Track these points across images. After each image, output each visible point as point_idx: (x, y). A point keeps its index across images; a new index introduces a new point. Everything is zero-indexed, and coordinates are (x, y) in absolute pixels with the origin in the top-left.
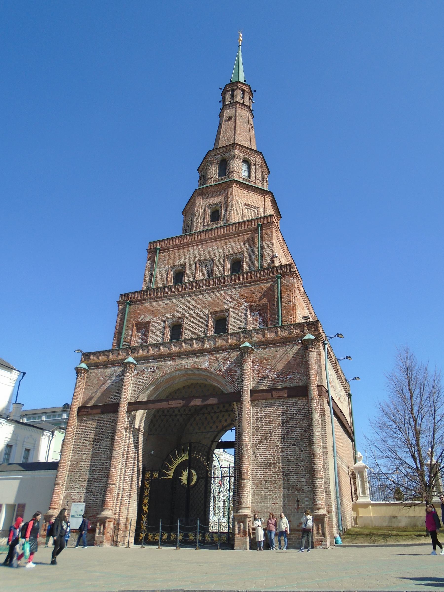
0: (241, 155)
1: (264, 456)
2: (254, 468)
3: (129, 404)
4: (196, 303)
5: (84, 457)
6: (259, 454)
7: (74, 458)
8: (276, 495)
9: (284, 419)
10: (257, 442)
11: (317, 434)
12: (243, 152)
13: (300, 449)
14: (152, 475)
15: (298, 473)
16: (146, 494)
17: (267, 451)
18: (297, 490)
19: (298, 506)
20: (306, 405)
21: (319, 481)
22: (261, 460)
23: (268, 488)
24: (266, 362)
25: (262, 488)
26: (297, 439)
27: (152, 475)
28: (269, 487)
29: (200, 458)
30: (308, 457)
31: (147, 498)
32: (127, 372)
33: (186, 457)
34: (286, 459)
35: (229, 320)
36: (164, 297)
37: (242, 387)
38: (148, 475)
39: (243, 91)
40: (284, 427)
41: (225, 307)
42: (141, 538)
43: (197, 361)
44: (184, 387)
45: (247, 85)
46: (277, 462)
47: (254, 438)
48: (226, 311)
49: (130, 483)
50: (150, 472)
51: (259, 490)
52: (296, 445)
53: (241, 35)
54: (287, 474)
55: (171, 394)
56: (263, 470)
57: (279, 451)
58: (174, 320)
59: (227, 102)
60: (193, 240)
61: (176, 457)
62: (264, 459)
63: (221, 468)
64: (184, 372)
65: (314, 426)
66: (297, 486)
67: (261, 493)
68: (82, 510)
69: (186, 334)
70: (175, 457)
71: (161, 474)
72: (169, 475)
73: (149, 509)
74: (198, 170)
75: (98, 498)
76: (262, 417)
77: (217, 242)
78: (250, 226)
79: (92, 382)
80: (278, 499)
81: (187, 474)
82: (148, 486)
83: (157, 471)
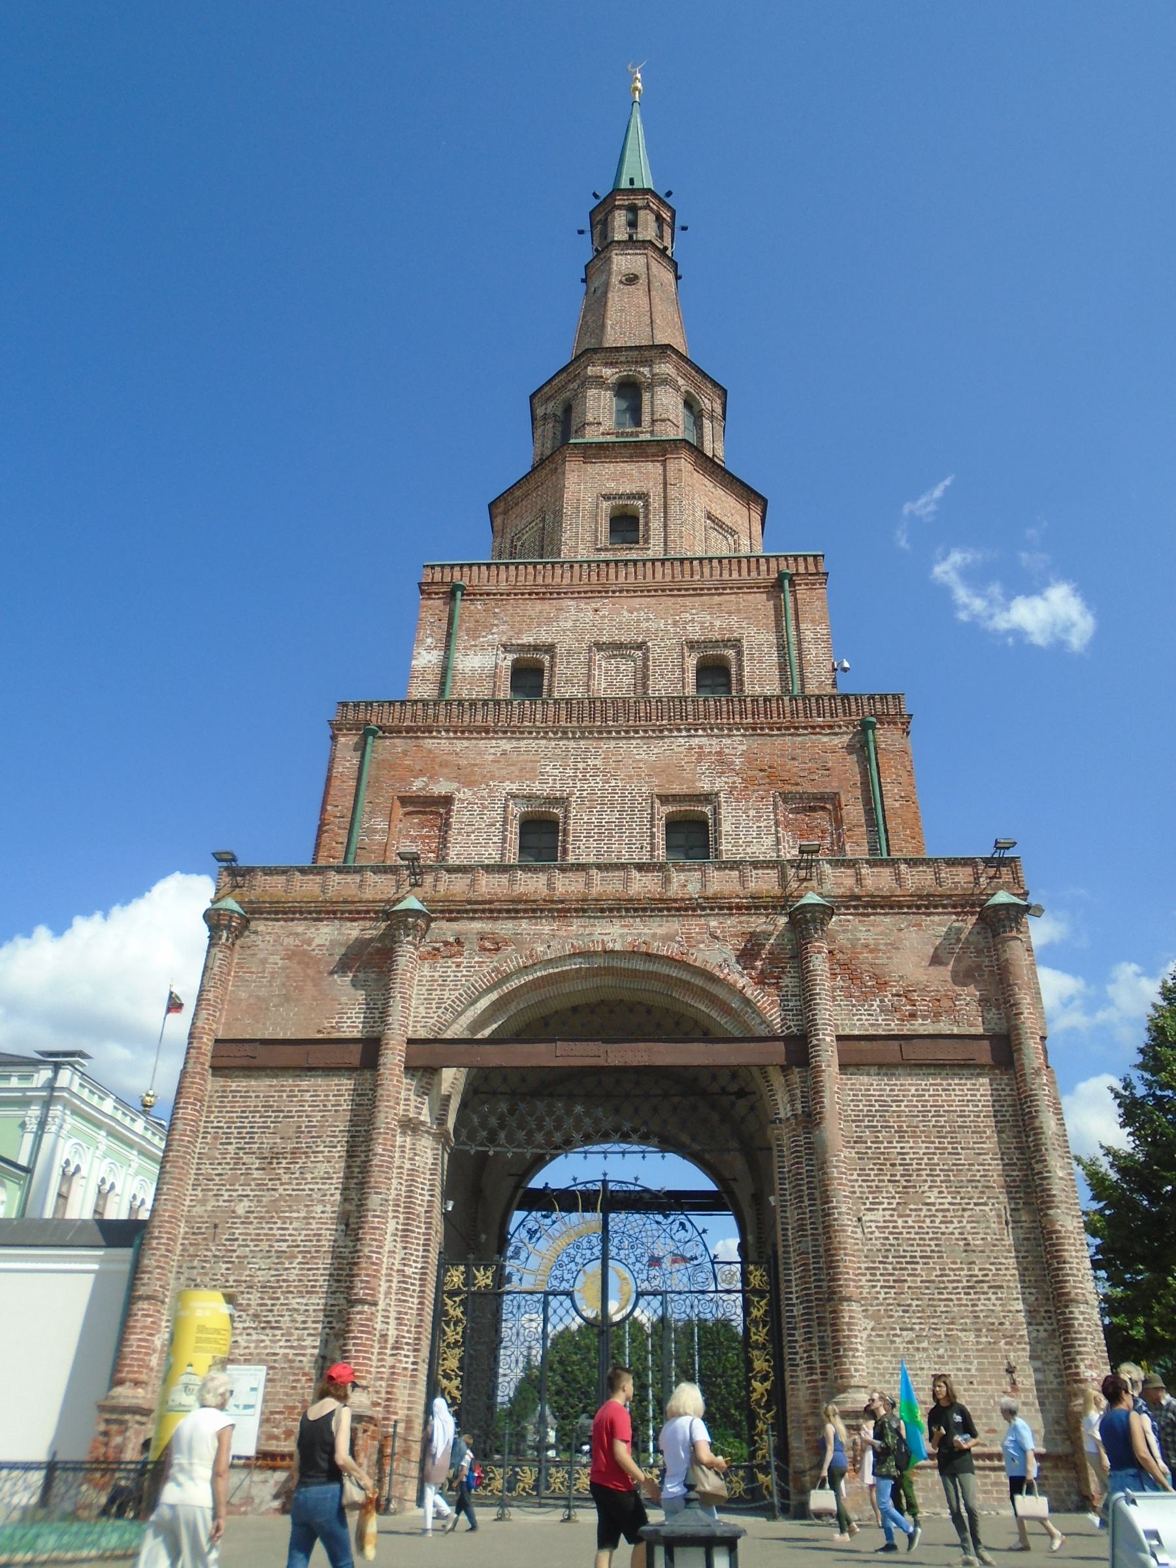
0: (681, 382)
1: (891, 1233)
2: (863, 1266)
3: (410, 1042)
4: (606, 764)
5: (241, 1209)
6: (873, 1225)
7: (199, 1210)
8: (941, 1351)
9: (943, 1127)
10: (866, 1190)
11: (1061, 1174)
12: (685, 376)
13: (999, 1216)
15: (1001, 1287)
17: (900, 1216)
18: (1005, 1337)
19: (1014, 1383)
20: (1003, 1090)
21: (1082, 1313)
22: (884, 1245)
23: (912, 1329)
24: (870, 956)
25: (895, 1329)
26: (987, 1187)
27: (469, 1279)
28: (917, 1327)
30: (1028, 1239)
31: (457, 1351)
32: (408, 942)
34: (962, 1243)
35: (717, 823)
36: (496, 732)
37: (812, 1022)
39: (659, 219)
40: (946, 1148)
41: (705, 786)
43: (646, 931)
44: (575, 1009)
45: (669, 208)
46: (932, 1251)
47: (855, 1177)
48: (707, 798)
49: (416, 1301)
50: (462, 1268)
51: (884, 1333)
52: (985, 1204)
53: (639, 76)
54: (969, 1287)
55: (528, 1025)
56: (892, 1275)
57: (938, 1220)
59: (620, 234)
60: (576, 581)
62: (892, 1242)
63: (713, 1263)
64: (599, 962)
65: (1051, 1151)
66: (1001, 1324)
67: (893, 1342)
68: (253, 1389)
69: (581, 846)
74: (532, 397)
75: (304, 1348)
76: (875, 1116)
77: (653, 601)
78: (754, 574)
79: (264, 962)
80: (947, 1364)
82: (458, 1312)
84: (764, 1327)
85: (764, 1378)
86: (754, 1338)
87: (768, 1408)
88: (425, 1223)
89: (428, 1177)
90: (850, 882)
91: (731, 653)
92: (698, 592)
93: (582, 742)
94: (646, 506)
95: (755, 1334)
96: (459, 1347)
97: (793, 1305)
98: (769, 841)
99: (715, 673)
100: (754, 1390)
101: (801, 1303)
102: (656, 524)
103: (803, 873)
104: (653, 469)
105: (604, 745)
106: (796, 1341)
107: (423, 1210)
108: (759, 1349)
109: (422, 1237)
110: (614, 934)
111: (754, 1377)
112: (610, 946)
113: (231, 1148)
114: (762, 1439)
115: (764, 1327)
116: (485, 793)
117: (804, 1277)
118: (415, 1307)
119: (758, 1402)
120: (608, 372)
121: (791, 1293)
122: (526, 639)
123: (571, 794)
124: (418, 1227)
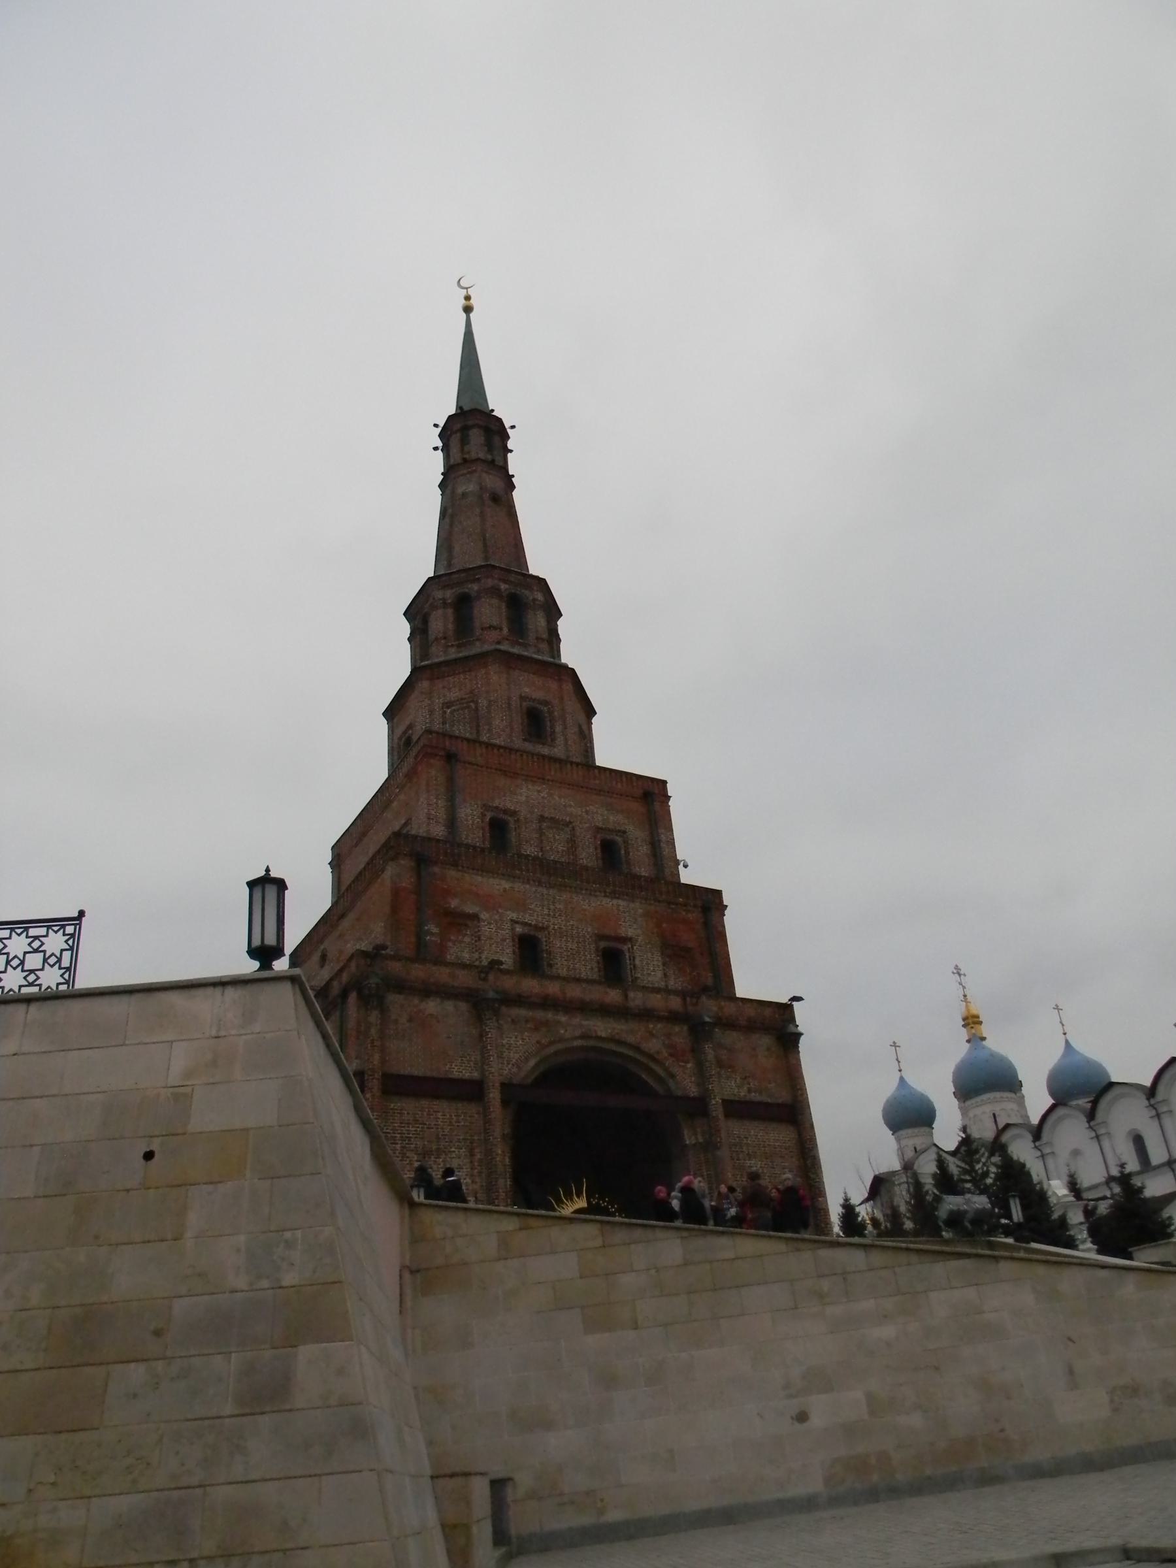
41: (622, 932)
58: (526, 930)
61: (563, 1202)
64: (591, 1043)
79: (396, 1021)
90: (715, 1009)
91: (619, 839)
92: (599, 792)
93: (551, 892)
94: (551, 713)
98: (659, 974)
99: (610, 850)
102: (558, 729)
103: (694, 1000)
104: (554, 685)
105: (565, 896)
110: (602, 1027)
112: (599, 1034)
113: (398, 1147)
116: (497, 917)
120: (503, 586)
122: (496, 803)
123: (548, 927)
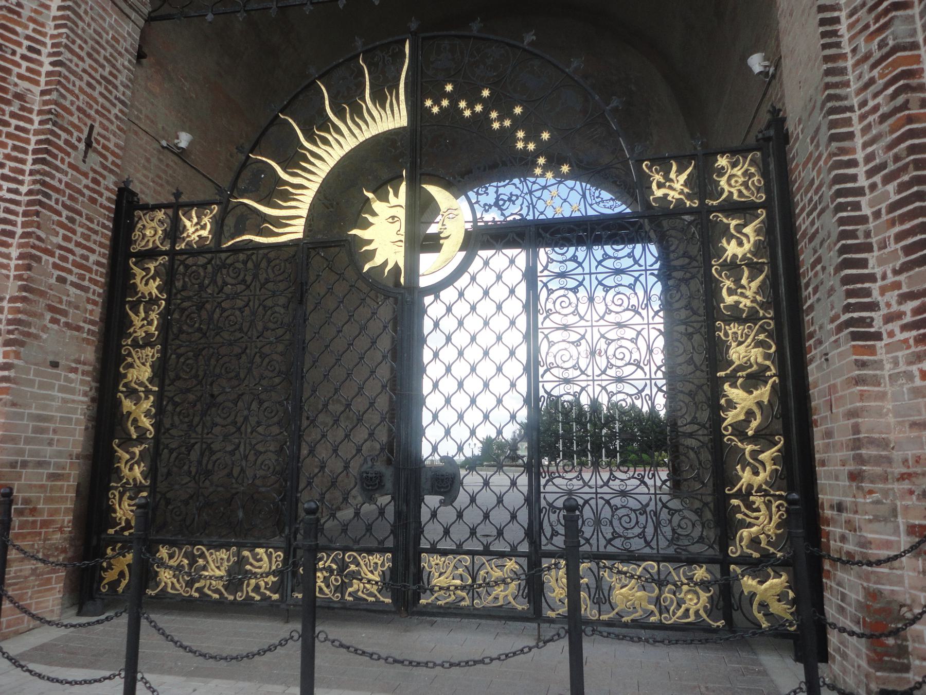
14: (175, 231)
16: (141, 334)
29: (486, 112)
31: (149, 351)
33: (391, 118)
38: (150, 231)
42: (110, 576)
49: (14, 252)
50: (160, 215)
61: (326, 124)
70: (316, 124)
71: (232, 219)
72: (278, 222)
73: (159, 414)
81: (401, 213)
82: (153, 287)
83: (202, 205)
84: (752, 279)
85: (754, 379)
86: (729, 300)
87: (763, 437)
88: (40, 112)
89: (50, 31)
95: (731, 292)
96: (152, 347)
97: (860, 192)
100: (731, 405)
101: (887, 180)
106: (872, 278)
107: (37, 90)
108: (740, 320)
109: (33, 139)
111: (732, 379)
114: (749, 506)
115: (752, 279)
117: (905, 106)
118: (13, 263)
119: (739, 429)
121: (853, 163)
124: (13, 115)
